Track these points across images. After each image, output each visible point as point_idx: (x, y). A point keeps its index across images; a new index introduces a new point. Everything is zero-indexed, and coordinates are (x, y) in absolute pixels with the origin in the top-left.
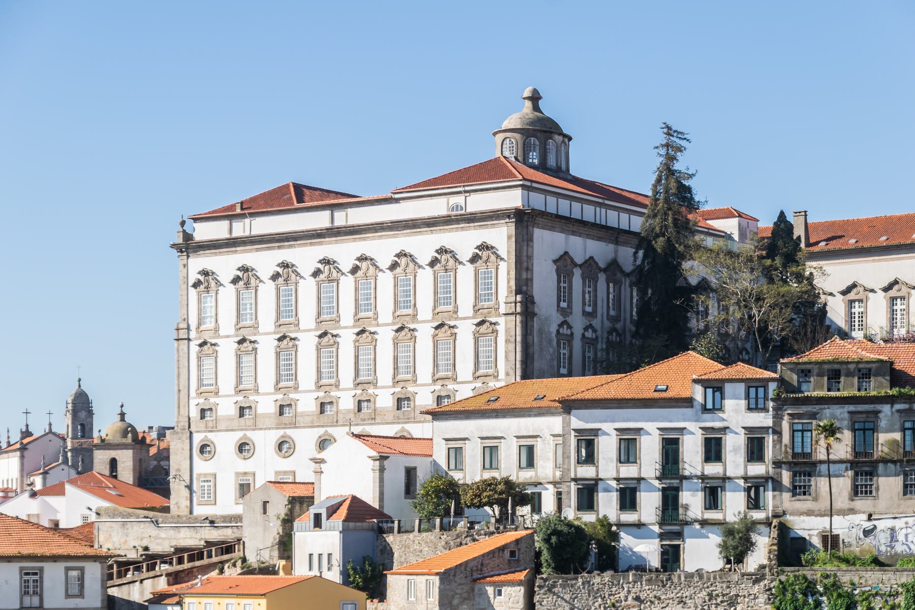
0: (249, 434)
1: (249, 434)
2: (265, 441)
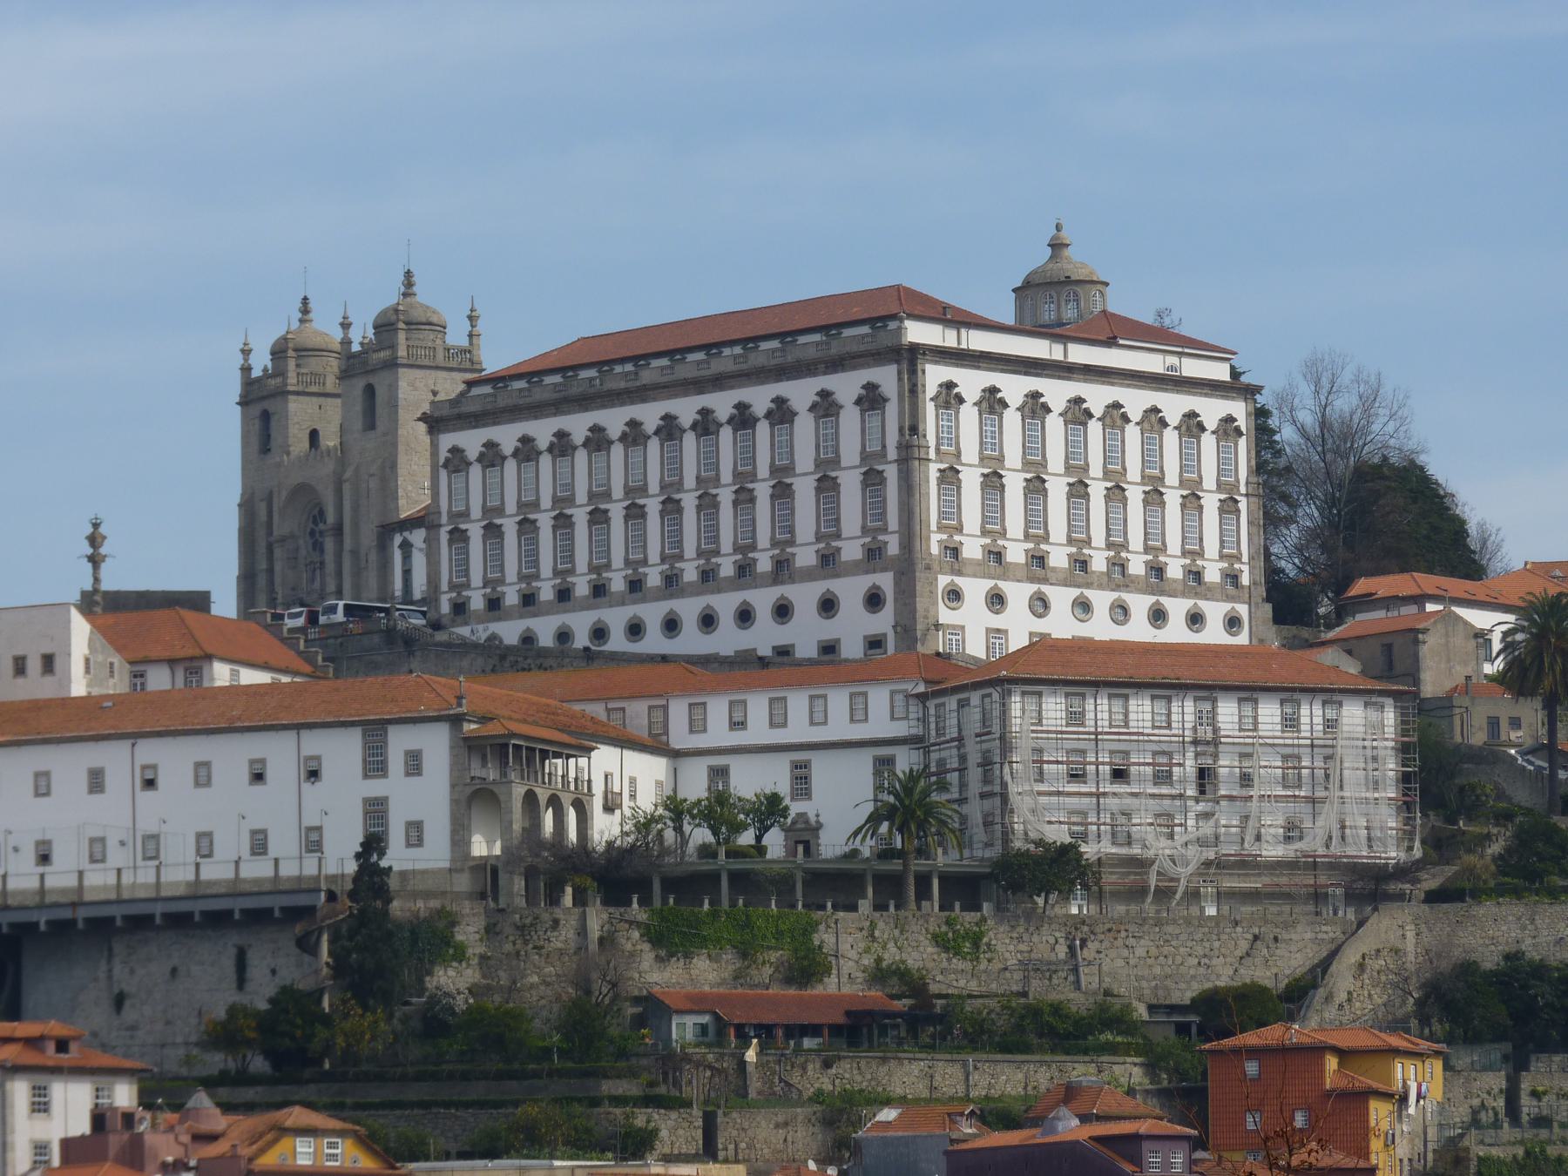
0: (1001, 584)
1: (1001, 584)
2: (1018, 593)
